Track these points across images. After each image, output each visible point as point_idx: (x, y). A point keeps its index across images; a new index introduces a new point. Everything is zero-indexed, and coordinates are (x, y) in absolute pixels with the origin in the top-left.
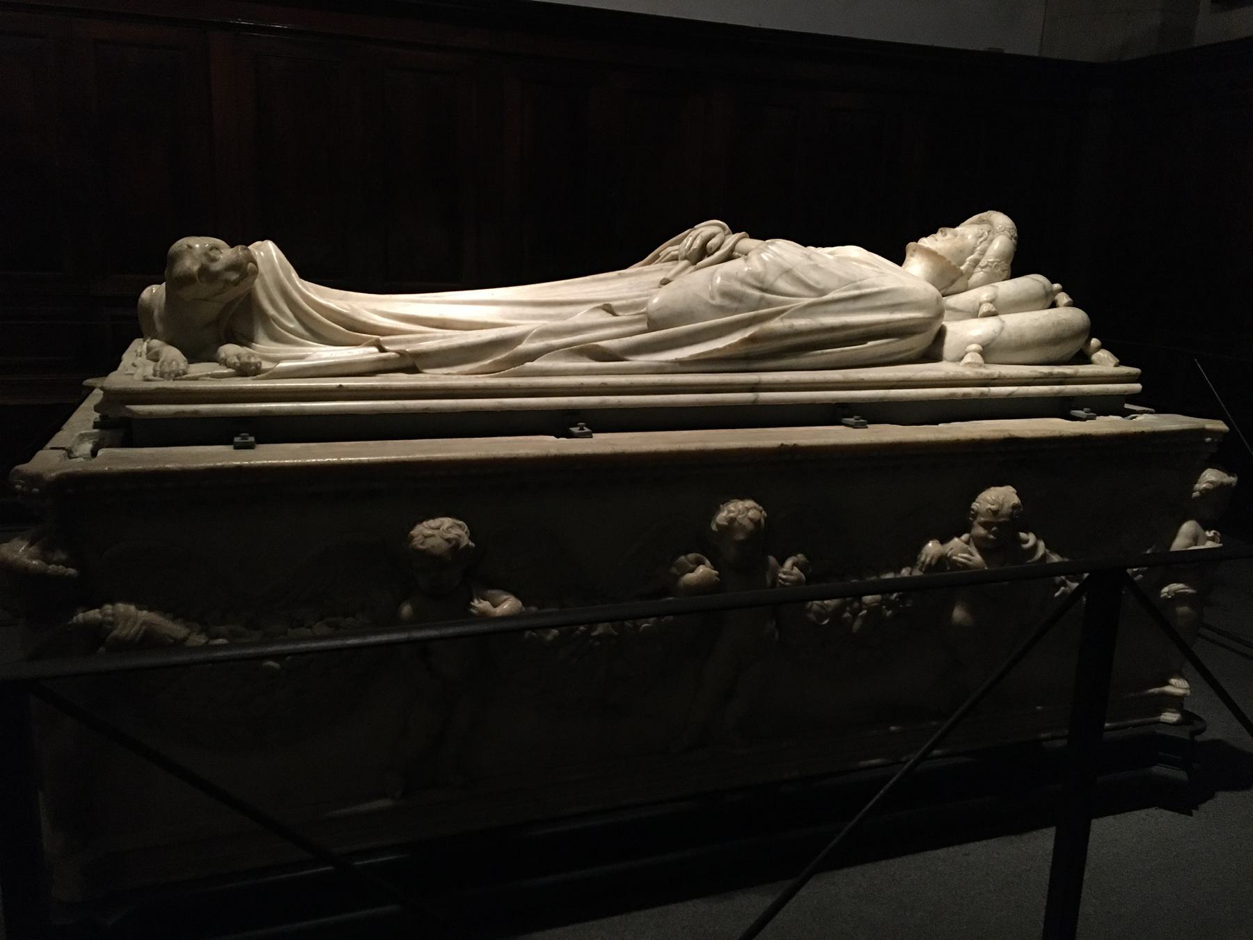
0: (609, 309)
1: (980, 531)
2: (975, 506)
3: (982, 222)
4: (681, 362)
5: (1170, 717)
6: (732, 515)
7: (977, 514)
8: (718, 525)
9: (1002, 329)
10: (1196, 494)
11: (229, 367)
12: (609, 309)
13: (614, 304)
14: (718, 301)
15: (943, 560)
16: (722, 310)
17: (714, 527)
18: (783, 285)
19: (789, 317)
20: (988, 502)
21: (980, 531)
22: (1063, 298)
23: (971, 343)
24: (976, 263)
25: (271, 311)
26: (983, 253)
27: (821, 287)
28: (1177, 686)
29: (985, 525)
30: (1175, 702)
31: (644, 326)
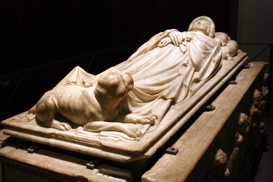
0: (185, 65)
1: (256, 102)
2: (255, 96)
3: (201, 19)
4: (209, 77)
5: (262, 131)
6: (244, 119)
7: (255, 98)
8: (242, 123)
9: (230, 49)
10: (264, 80)
11: (144, 123)
12: (185, 65)
13: (185, 62)
14: (203, 56)
15: (254, 112)
16: (204, 58)
17: (240, 124)
18: (209, 48)
19: (214, 57)
20: (257, 95)
21: (256, 102)
22: (229, 38)
23: (226, 54)
24: (209, 31)
25: (132, 97)
26: (210, 28)
27: (213, 46)
28: (262, 124)
29: (257, 101)
30: (262, 127)
31: (193, 69)
